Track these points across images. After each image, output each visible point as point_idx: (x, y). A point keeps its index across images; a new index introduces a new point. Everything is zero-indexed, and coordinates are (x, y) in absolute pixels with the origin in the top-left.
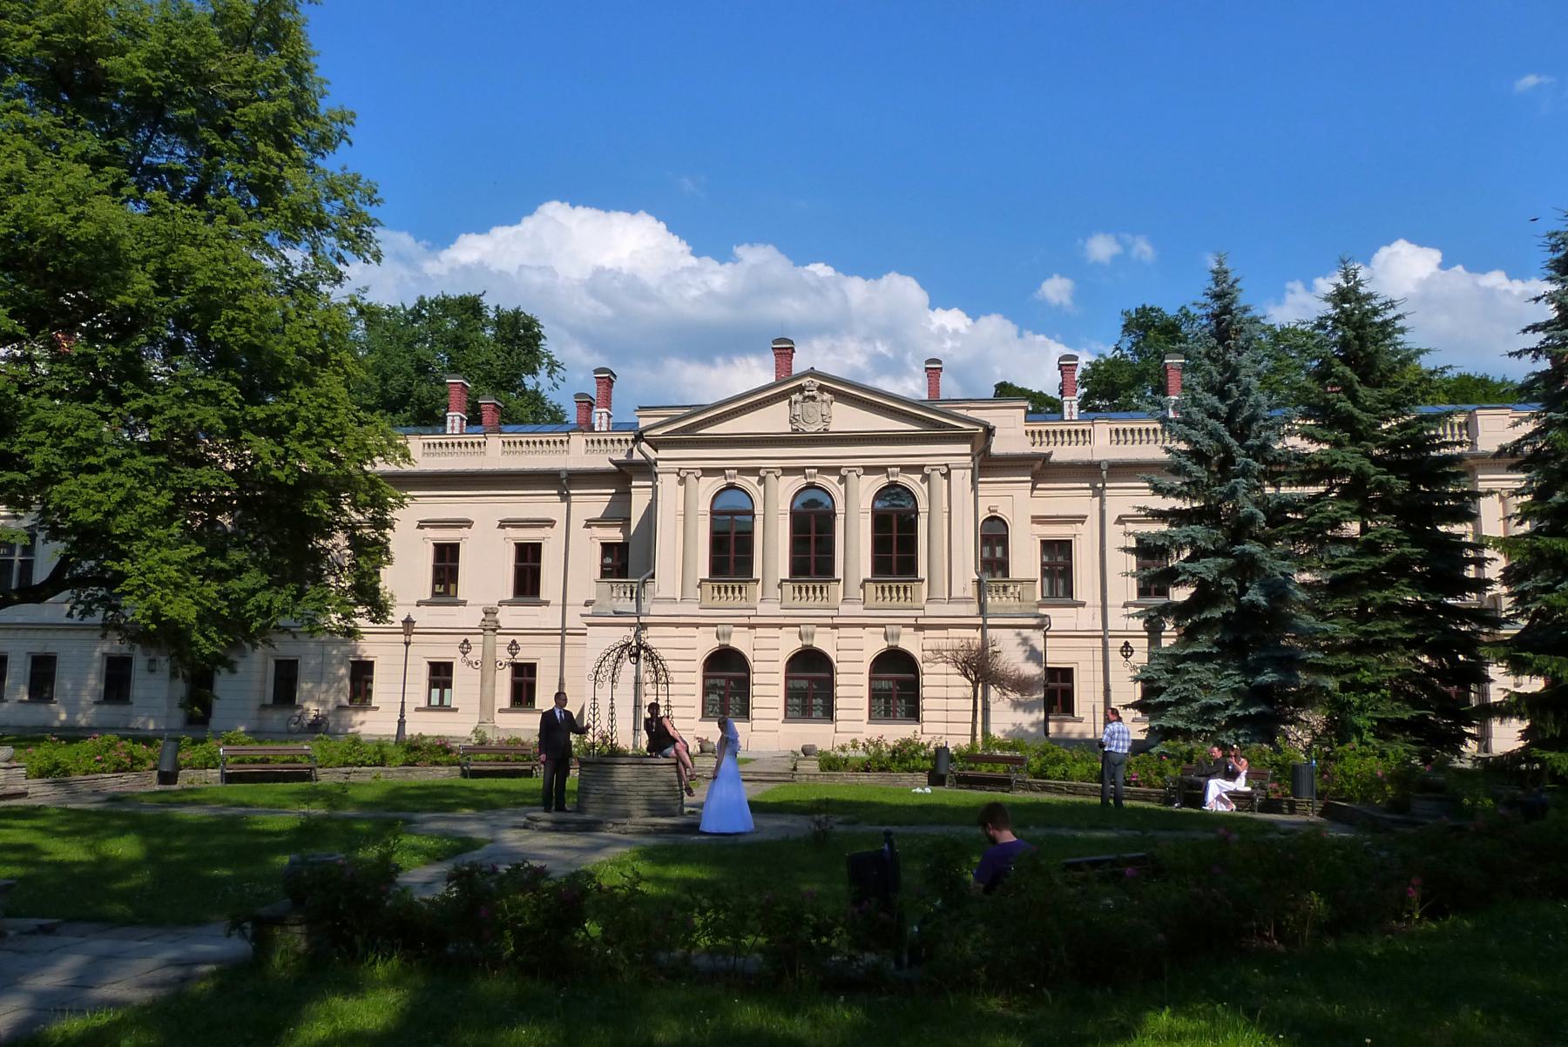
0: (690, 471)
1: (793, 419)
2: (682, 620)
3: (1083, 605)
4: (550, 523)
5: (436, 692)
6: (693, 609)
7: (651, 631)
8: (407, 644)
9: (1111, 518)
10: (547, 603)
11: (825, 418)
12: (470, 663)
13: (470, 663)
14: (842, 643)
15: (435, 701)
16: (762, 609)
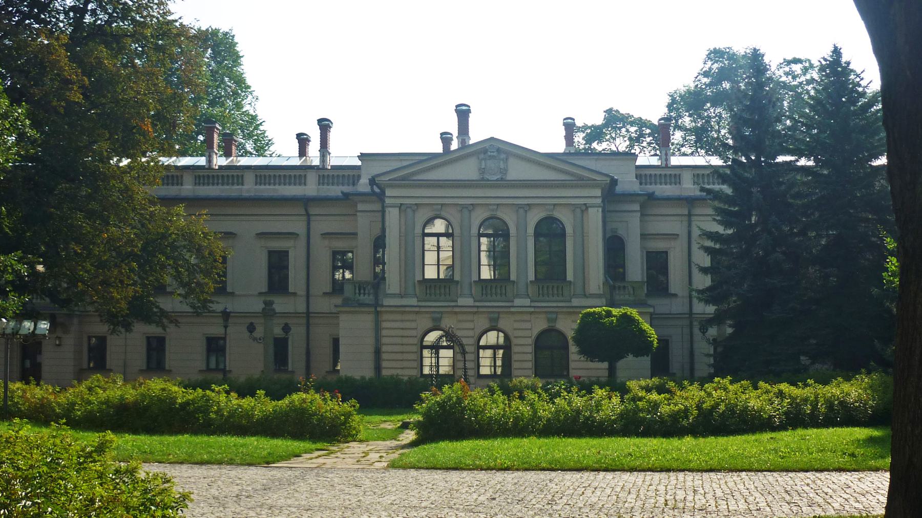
0: (409, 206)
1: (482, 171)
2: (407, 309)
3: (675, 295)
4: (293, 235)
5: (213, 360)
6: (413, 301)
7: (385, 317)
8: (226, 327)
9: (696, 232)
10: (294, 294)
11: (505, 171)
12: (255, 339)
13: (255, 339)
14: (517, 325)
15: (213, 365)
16: (462, 301)
